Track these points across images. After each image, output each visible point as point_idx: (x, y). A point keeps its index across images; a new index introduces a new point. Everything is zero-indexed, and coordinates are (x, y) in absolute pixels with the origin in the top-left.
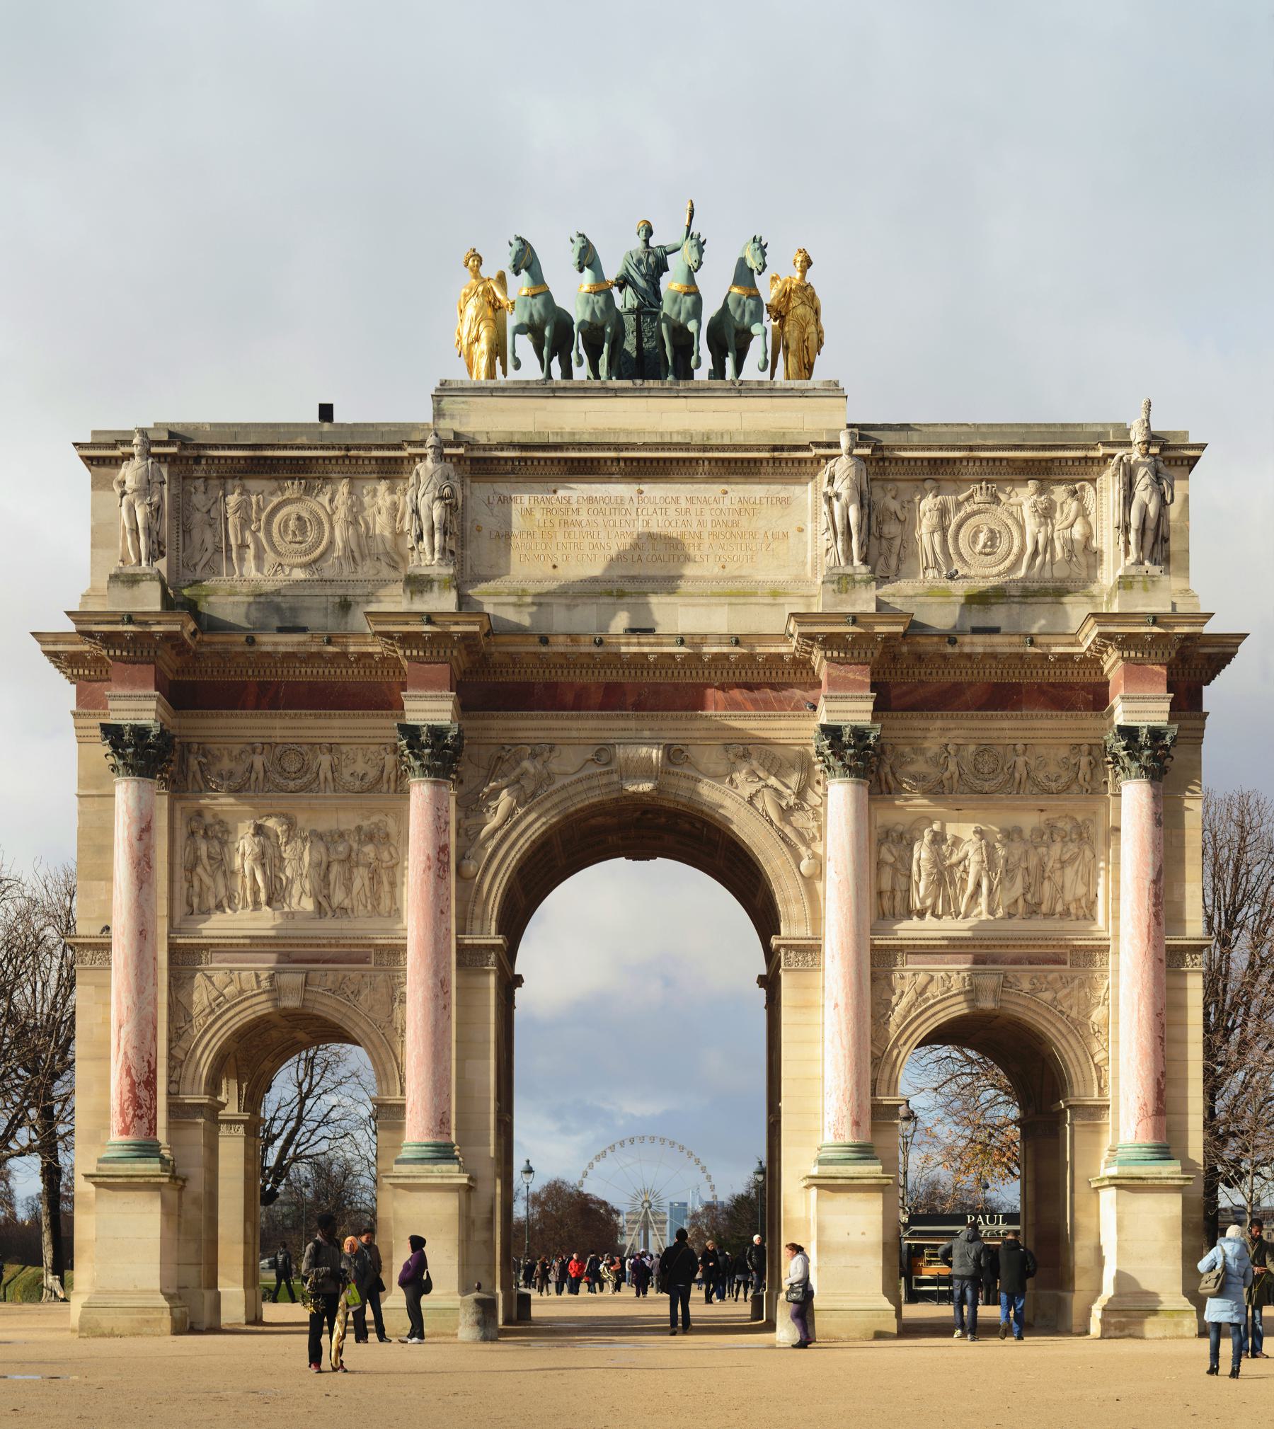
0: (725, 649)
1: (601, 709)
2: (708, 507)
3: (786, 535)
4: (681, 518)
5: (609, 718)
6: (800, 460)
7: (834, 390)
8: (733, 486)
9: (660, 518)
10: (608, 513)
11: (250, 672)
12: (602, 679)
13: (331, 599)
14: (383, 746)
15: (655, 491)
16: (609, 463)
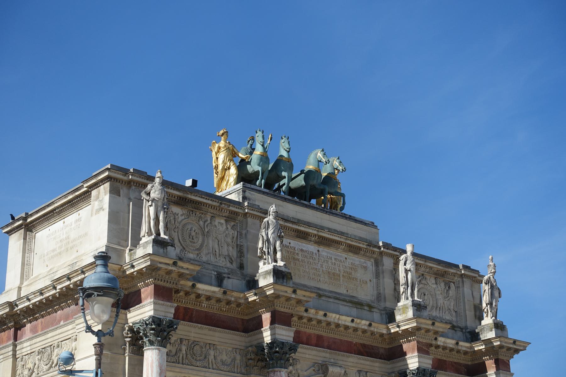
0: (366, 328)
1: (316, 346)
2: (341, 264)
3: (366, 282)
4: (333, 266)
5: (320, 351)
6: (374, 252)
7: (376, 226)
8: (349, 256)
9: (326, 265)
10: (308, 258)
11: (184, 302)
12: (317, 332)
13: (213, 272)
14: (235, 349)
15: (325, 251)
16: (313, 236)
